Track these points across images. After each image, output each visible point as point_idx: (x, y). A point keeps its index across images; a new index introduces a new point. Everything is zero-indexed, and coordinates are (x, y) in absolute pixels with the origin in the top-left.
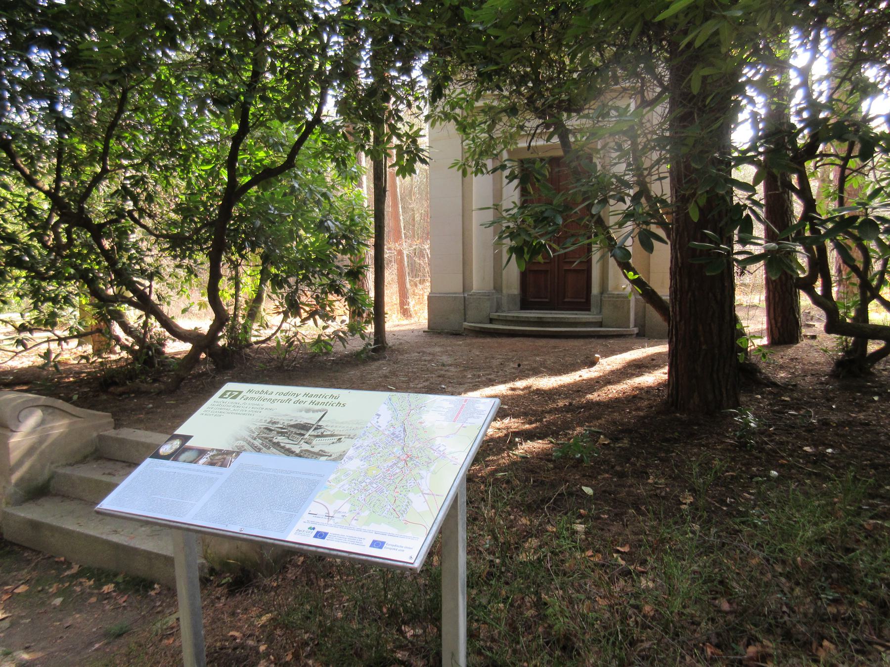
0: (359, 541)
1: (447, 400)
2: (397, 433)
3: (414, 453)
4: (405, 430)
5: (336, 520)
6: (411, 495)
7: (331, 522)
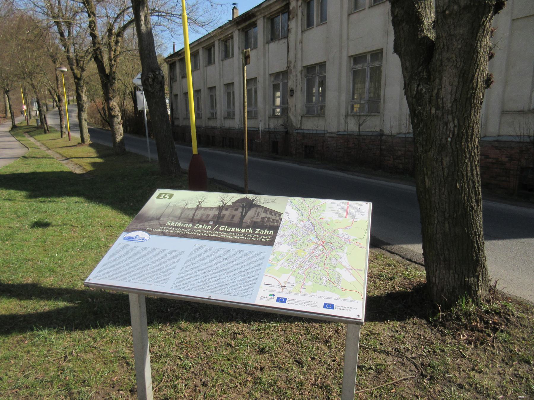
1: (334, 203)
2: (308, 226)
3: (327, 240)
4: (312, 224)
5: (289, 289)
6: (338, 270)
7: (285, 290)
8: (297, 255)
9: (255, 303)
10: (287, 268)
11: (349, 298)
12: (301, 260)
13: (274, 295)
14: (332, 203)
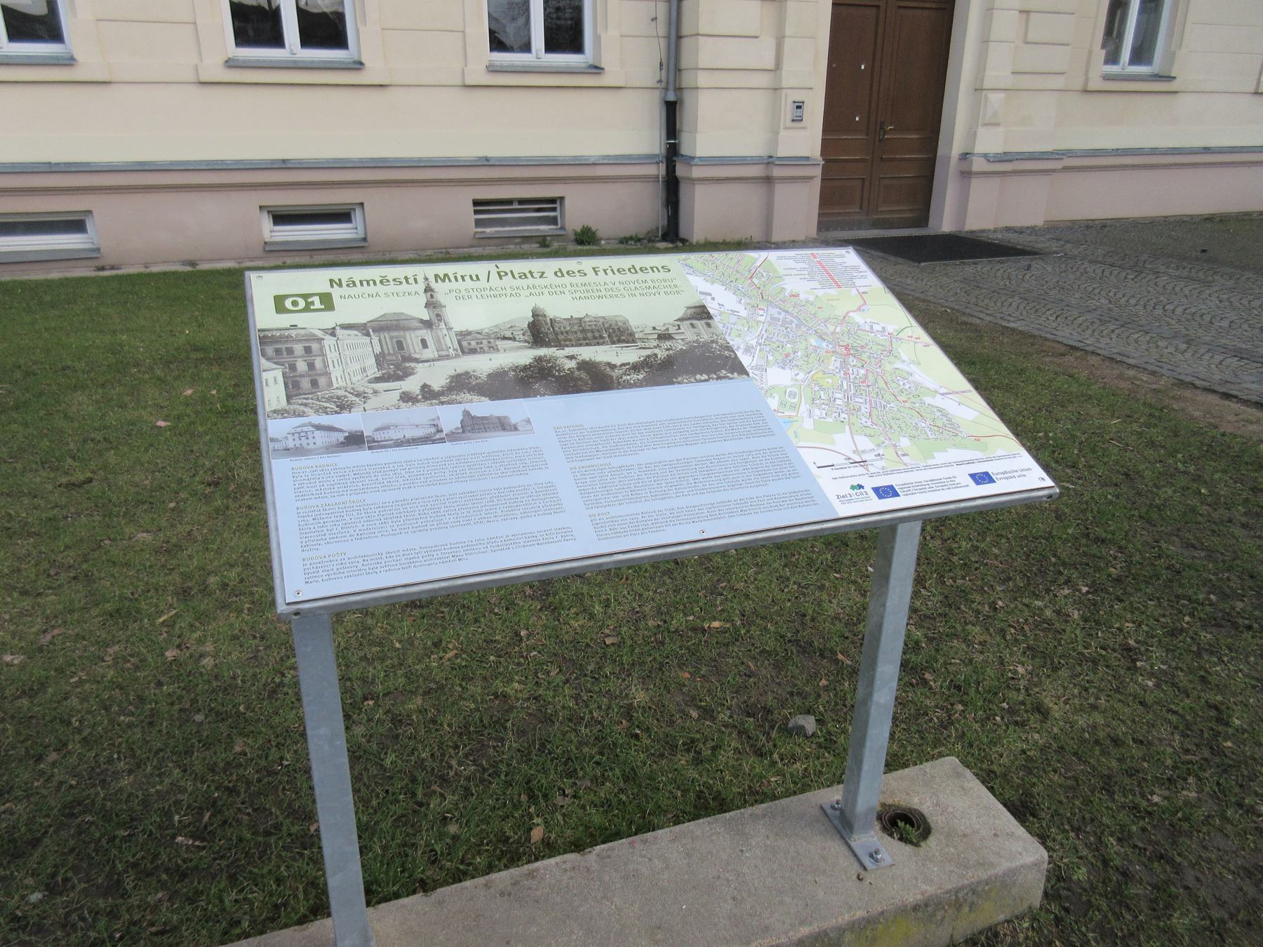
0: (951, 483)
4: (787, 312)
6: (928, 400)
8: (822, 389)
10: (829, 420)
11: (1000, 452)
12: (837, 395)
13: (861, 487)
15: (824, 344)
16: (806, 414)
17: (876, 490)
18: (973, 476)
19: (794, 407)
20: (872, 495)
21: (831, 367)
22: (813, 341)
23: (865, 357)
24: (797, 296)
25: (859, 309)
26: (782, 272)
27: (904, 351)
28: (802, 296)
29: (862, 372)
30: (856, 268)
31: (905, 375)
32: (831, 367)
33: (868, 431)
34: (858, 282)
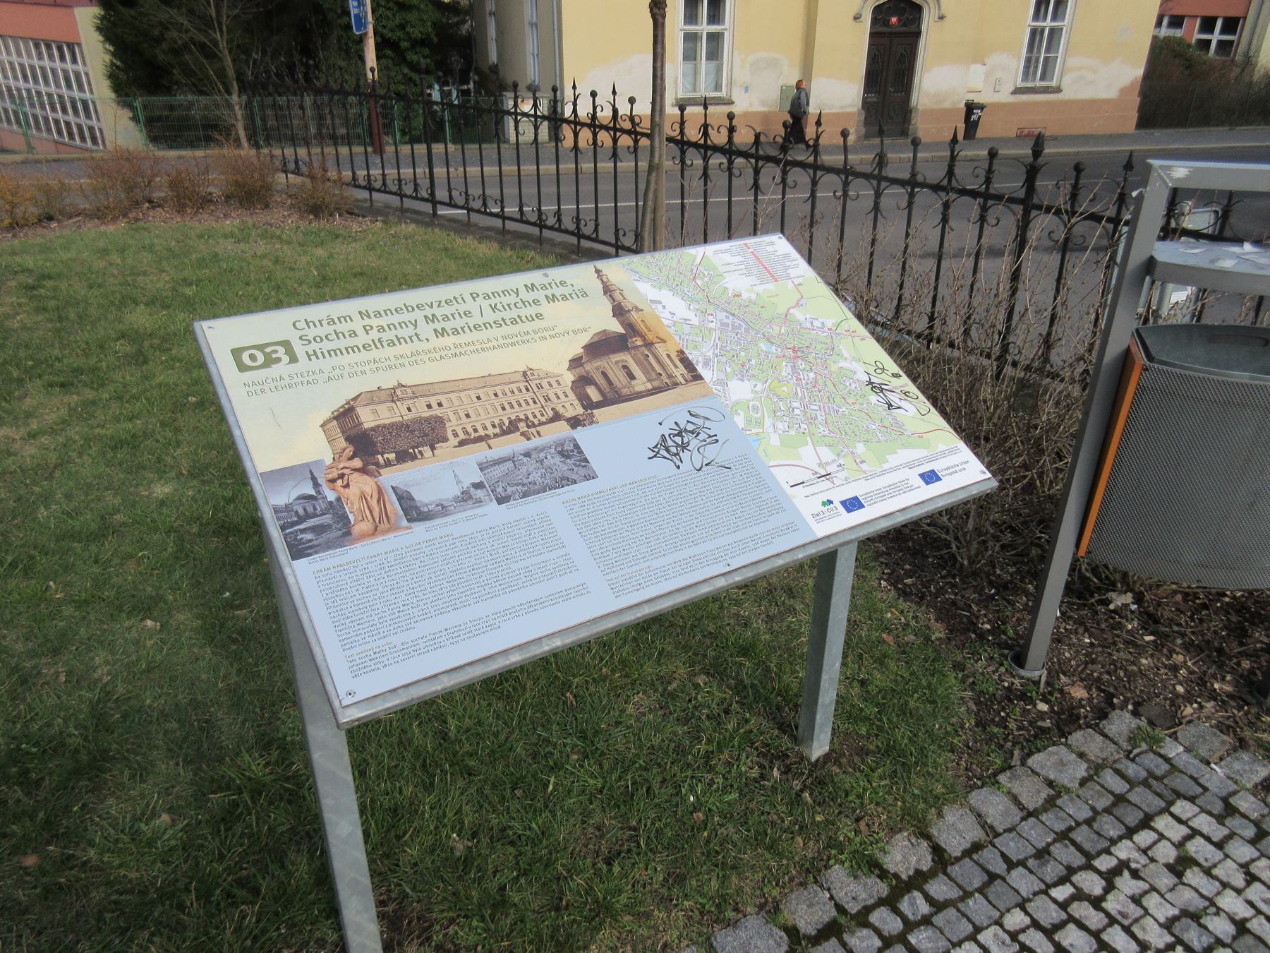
2: (729, 321)
4: (733, 315)
9: (820, 535)
10: (792, 433)
11: (942, 447)
12: (795, 405)
13: (830, 502)
14: (716, 252)
15: (773, 348)
16: (771, 430)
17: (844, 503)
18: (922, 476)
19: (759, 423)
20: (841, 509)
21: (784, 374)
22: (763, 346)
23: (811, 358)
24: (739, 296)
25: (798, 305)
26: (721, 269)
27: (844, 347)
28: (745, 295)
29: (812, 375)
30: (787, 256)
31: (849, 374)
32: (784, 374)
33: (828, 441)
34: (792, 273)
